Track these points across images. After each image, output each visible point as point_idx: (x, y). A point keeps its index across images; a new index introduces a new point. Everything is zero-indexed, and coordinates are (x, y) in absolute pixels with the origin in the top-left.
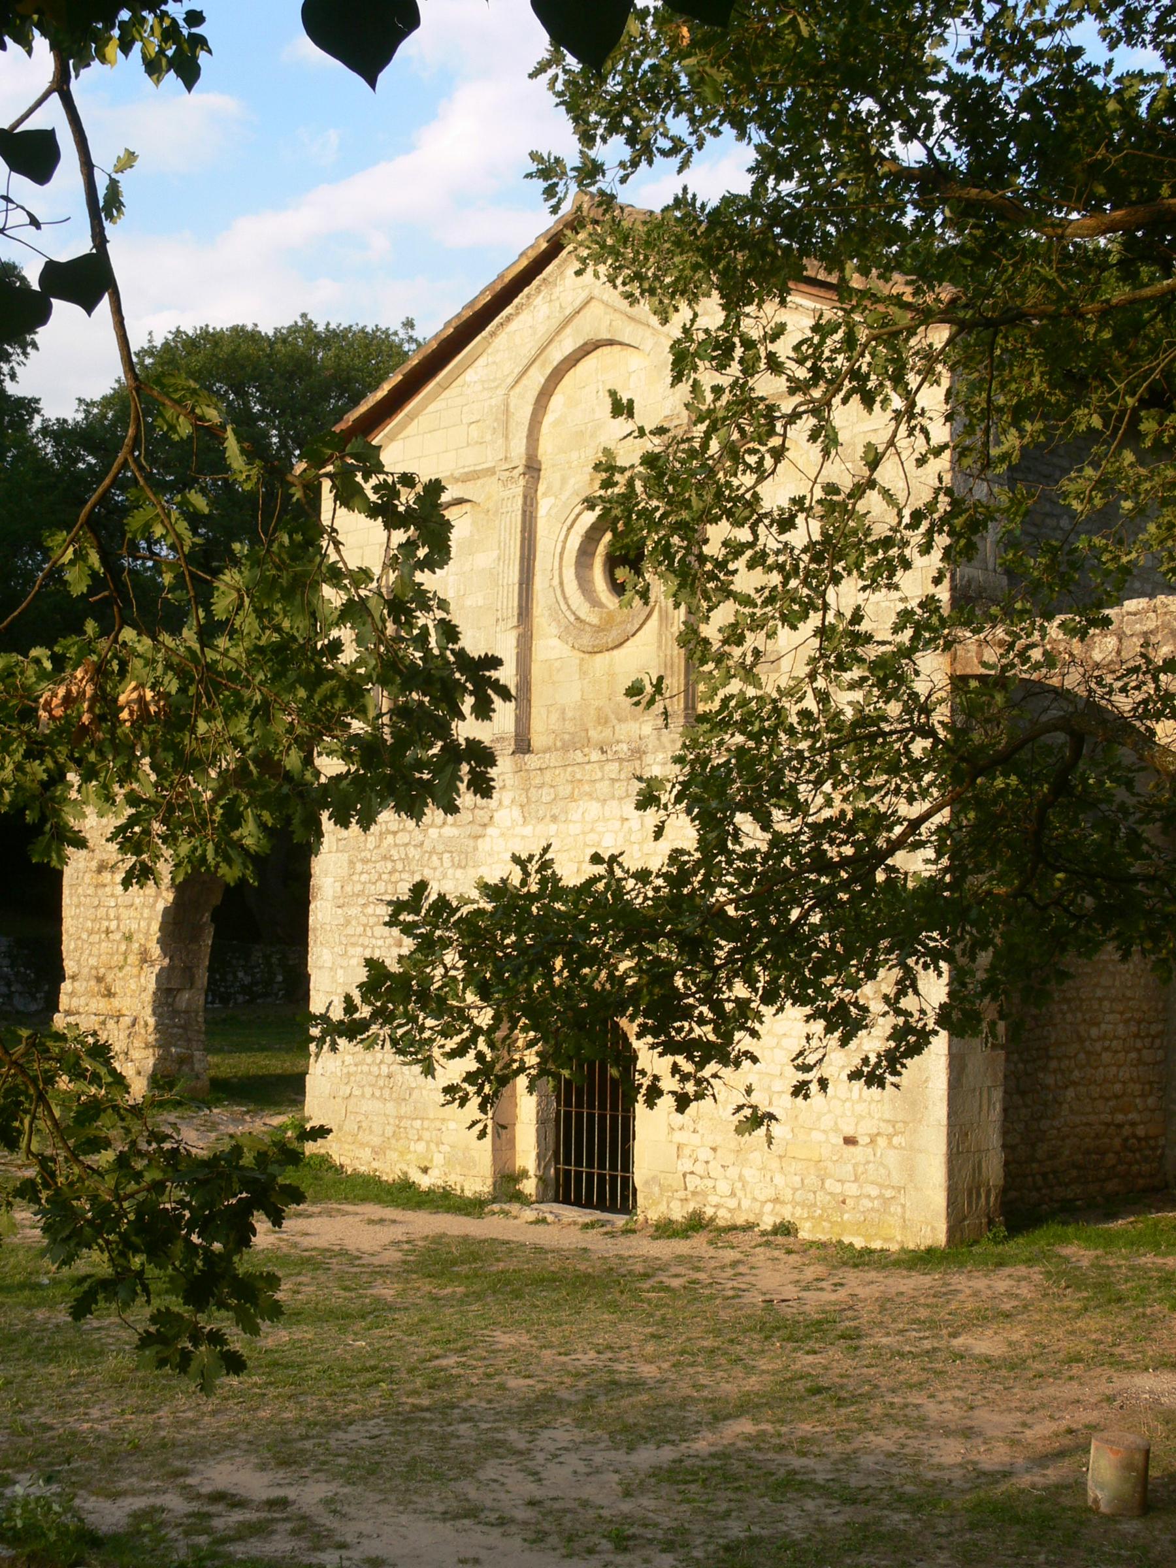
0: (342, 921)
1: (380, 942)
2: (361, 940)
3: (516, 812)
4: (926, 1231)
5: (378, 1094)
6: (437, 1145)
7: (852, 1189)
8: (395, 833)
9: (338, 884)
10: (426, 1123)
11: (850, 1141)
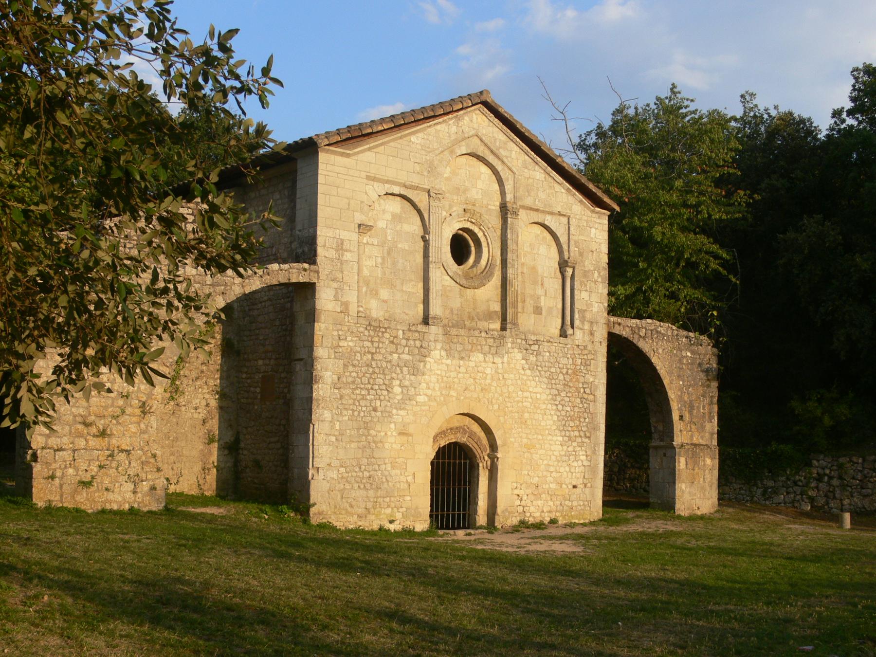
0: (339, 396)
1: (364, 409)
3: (443, 353)
4: (596, 514)
5: (362, 486)
6: (398, 509)
7: (575, 503)
8: (372, 354)
9: (335, 377)
10: (392, 499)
11: (575, 487)
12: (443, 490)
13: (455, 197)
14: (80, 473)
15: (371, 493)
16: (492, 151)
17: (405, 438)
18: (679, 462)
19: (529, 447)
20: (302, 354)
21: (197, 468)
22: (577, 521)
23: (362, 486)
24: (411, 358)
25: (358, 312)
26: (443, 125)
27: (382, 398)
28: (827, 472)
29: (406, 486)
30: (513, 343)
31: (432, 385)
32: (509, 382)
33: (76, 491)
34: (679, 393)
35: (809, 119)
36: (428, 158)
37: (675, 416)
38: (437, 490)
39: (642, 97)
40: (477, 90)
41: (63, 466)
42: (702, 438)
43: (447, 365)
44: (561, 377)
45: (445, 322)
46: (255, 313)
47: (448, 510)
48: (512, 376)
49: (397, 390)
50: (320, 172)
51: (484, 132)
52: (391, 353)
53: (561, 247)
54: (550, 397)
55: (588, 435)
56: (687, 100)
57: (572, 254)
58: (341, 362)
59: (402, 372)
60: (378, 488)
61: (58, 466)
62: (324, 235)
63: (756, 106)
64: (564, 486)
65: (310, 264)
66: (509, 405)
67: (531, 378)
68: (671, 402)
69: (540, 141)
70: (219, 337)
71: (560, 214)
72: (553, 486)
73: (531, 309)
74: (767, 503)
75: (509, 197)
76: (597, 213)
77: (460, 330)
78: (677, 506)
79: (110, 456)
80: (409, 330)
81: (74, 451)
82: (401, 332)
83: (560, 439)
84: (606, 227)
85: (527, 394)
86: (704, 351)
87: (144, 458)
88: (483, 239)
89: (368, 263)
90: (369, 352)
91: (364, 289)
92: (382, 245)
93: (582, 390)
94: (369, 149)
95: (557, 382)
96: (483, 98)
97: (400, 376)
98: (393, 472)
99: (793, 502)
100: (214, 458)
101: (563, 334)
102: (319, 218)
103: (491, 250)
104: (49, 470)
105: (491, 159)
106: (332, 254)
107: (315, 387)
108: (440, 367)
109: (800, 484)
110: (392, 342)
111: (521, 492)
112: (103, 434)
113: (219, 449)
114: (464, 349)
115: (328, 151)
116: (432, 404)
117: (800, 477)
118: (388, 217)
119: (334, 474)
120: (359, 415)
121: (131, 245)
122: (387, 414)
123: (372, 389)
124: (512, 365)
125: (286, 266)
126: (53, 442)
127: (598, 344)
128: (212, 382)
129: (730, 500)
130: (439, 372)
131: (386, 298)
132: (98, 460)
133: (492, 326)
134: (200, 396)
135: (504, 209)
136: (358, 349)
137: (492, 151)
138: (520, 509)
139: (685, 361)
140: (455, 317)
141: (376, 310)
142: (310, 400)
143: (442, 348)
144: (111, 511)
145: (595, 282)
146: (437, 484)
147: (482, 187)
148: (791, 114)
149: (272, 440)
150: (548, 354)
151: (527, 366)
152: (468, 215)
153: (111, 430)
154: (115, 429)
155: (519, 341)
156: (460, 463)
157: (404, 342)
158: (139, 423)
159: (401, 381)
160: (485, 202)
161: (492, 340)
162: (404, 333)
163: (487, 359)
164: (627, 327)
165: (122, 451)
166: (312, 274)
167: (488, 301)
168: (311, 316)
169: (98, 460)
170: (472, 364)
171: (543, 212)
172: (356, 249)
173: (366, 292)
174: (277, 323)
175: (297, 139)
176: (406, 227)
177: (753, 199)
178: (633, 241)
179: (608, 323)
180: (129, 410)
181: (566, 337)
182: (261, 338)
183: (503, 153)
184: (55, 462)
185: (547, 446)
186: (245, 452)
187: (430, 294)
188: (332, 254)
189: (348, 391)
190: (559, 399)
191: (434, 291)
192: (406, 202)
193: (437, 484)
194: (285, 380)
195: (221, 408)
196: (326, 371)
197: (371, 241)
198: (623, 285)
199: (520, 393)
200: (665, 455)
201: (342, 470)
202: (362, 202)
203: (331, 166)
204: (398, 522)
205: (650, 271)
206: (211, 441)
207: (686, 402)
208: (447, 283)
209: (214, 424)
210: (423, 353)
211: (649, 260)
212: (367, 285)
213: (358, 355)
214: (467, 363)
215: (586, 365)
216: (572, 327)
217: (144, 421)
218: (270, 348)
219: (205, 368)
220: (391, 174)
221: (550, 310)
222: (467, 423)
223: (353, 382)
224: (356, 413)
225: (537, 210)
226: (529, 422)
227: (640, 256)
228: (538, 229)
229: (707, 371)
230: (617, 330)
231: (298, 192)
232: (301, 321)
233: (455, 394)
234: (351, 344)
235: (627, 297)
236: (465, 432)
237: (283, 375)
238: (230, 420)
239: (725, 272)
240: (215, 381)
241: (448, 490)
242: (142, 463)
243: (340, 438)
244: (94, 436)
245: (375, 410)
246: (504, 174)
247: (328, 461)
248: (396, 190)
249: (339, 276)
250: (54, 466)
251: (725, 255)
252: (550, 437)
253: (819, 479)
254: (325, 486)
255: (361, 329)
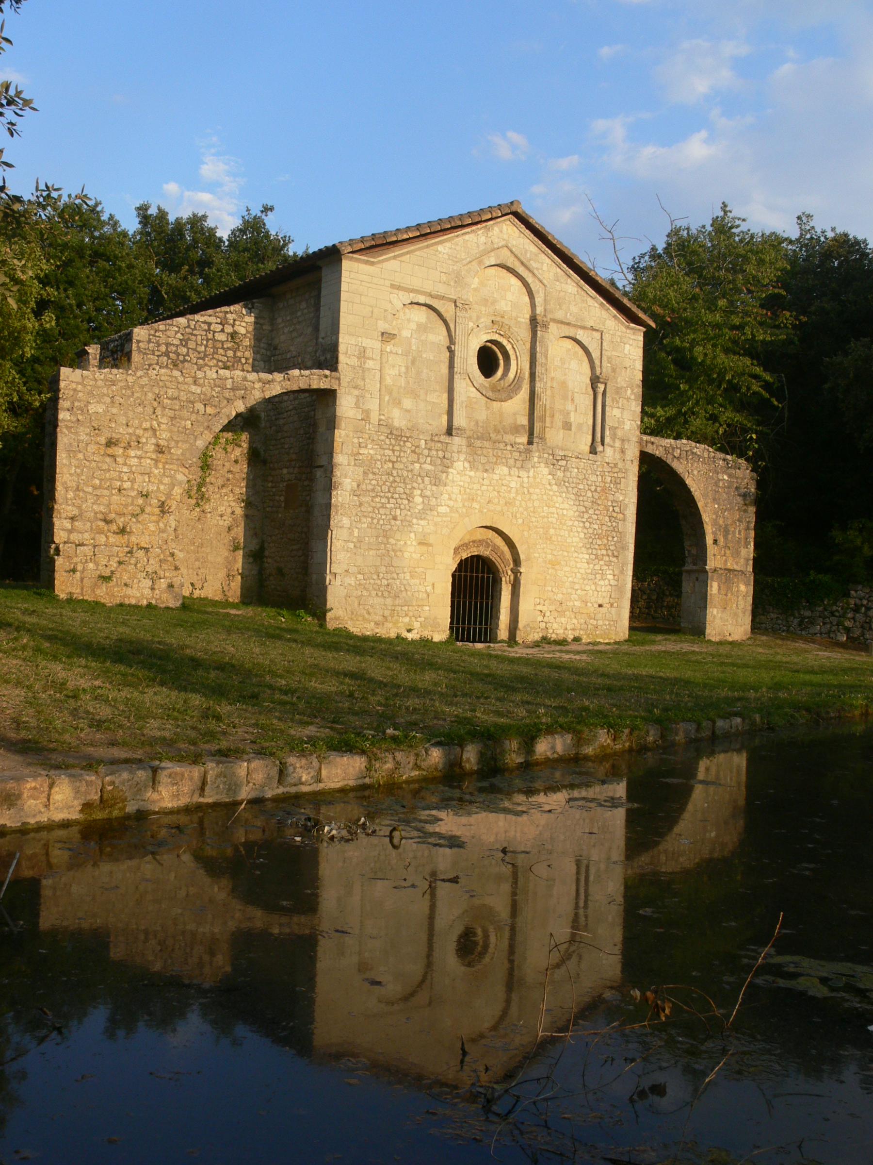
1: (384, 517)
2: (371, 515)
3: (467, 465)
5: (380, 594)
7: (600, 623)
8: (393, 462)
9: (355, 484)
10: (410, 608)
11: (600, 606)
12: (464, 603)
13: (483, 309)
14: (100, 567)
15: (389, 601)
16: (522, 263)
17: (425, 548)
18: (711, 586)
19: (554, 564)
20: (323, 461)
21: (222, 574)
22: (601, 641)
23: (380, 594)
24: (433, 468)
25: (380, 420)
26: (472, 235)
27: (402, 507)
28: (865, 602)
29: (425, 596)
30: (539, 457)
31: (454, 496)
32: (535, 497)
33: (96, 585)
34: (714, 517)
35: (865, 241)
36: (455, 268)
37: (709, 540)
38: (459, 603)
39: (698, 219)
40: (507, 200)
41: (84, 561)
42: (737, 563)
43: (470, 477)
44: (589, 494)
45: (469, 433)
46: (281, 422)
47: (469, 623)
48: (538, 491)
49: (418, 500)
50: (343, 279)
51: (514, 243)
52: (413, 463)
53: (593, 363)
54: (577, 514)
55: (616, 554)
56: (739, 219)
57: (604, 370)
58: (362, 469)
59: (423, 482)
60: (396, 597)
61: (79, 560)
62: (346, 342)
63: (813, 228)
64: (589, 604)
65: (331, 371)
66: (534, 519)
67: (557, 494)
68: (705, 526)
69: (572, 254)
70: (245, 445)
71: (592, 329)
72: (577, 604)
73: (560, 424)
74: (803, 633)
75: (539, 310)
76: (632, 329)
77: (485, 443)
78: (708, 631)
79: (129, 552)
80: (432, 440)
81: (95, 546)
82: (423, 442)
83: (587, 556)
84: (641, 344)
85: (554, 510)
86: (742, 474)
87: (162, 556)
88: (511, 352)
89: (391, 373)
90: (390, 461)
91: (387, 398)
92: (406, 354)
93: (611, 509)
94: (394, 258)
95: (585, 499)
96: (514, 209)
97: (422, 486)
98: (412, 582)
99: (829, 632)
100: (239, 565)
101: (593, 451)
102: (341, 326)
103: (519, 363)
104: (70, 563)
105: (521, 270)
106: (354, 361)
107: (334, 493)
108: (463, 478)
109: (837, 614)
110: (414, 452)
111: (544, 608)
112: (122, 531)
113: (244, 556)
114: (488, 462)
115: (351, 259)
116: (453, 515)
117: (838, 608)
118: (413, 326)
119: (351, 581)
120: (378, 523)
121: (160, 353)
122: (407, 524)
123: (392, 497)
124: (538, 480)
125: (307, 372)
126: (75, 537)
127: (629, 463)
128: (237, 491)
129: (766, 629)
130: (462, 483)
131: (409, 408)
132: (117, 556)
133: (518, 440)
134: (226, 503)
135: (534, 321)
136: (379, 458)
137: (522, 263)
138: (543, 625)
139: (721, 484)
140: (480, 430)
141: (398, 420)
142: (329, 505)
143: (465, 459)
144: (130, 606)
145: (628, 399)
146: (459, 597)
147: (511, 299)
148: (846, 235)
149: (295, 547)
150: (576, 470)
151: (553, 482)
152: (496, 327)
153: (131, 528)
154: (135, 527)
155: (546, 455)
156: (483, 577)
157: (426, 452)
158: (158, 522)
159: (422, 491)
160: (514, 314)
161: (518, 454)
162: (426, 443)
163: (512, 473)
164: (660, 446)
165: (141, 548)
166: (333, 381)
167: (515, 414)
168: (332, 423)
169: (117, 556)
170: (496, 477)
171: (575, 326)
172: (379, 358)
173: (388, 402)
174: (302, 432)
175: (322, 247)
176: (431, 337)
177: (800, 320)
178: (675, 362)
179: (640, 442)
180: (148, 509)
181: (596, 453)
182: (286, 446)
183: (533, 265)
184: (76, 556)
185: (572, 563)
186: (269, 560)
187: (455, 405)
188: (354, 361)
189: (368, 499)
190: (586, 516)
191: (458, 402)
192: (432, 312)
193: (459, 597)
194: (308, 488)
195: (246, 516)
196: (346, 478)
197: (394, 350)
198: (663, 407)
199: (545, 508)
200: (697, 580)
201: (360, 577)
202: (386, 311)
203: (354, 274)
204: (415, 631)
205: (691, 393)
206: (236, 548)
207: (721, 526)
208: (472, 395)
209: (239, 532)
210: (446, 464)
211: (690, 381)
212: (390, 394)
213: (379, 463)
214: (491, 475)
215: (616, 483)
216: (603, 444)
217: (163, 520)
218: (294, 457)
219: (231, 476)
220: (416, 283)
221: (580, 426)
222: (490, 537)
223: (373, 490)
224: (375, 521)
225: (568, 324)
226: (554, 538)
227: (683, 377)
228: (569, 344)
229: (744, 496)
230: (650, 449)
231: (322, 300)
232: (322, 429)
233: (477, 507)
234: (371, 452)
235: (669, 420)
236: (488, 545)
237: (306, 483)
238: (255, 528)
239: (767, 395)
240: (241, 489)
241: (470, 603)
242: (160, 561)
243: (358, 545)
244: (114, 533)
245: (395, 518)
246: (535, 286)
247: (346, 567)
248: (422, 299)
249: (361, 383)
250: (75, 560)
251: (768, 378)
252: (576, 555)
253: (856, 609)
254: (342, 592)
255: (382, 438)
